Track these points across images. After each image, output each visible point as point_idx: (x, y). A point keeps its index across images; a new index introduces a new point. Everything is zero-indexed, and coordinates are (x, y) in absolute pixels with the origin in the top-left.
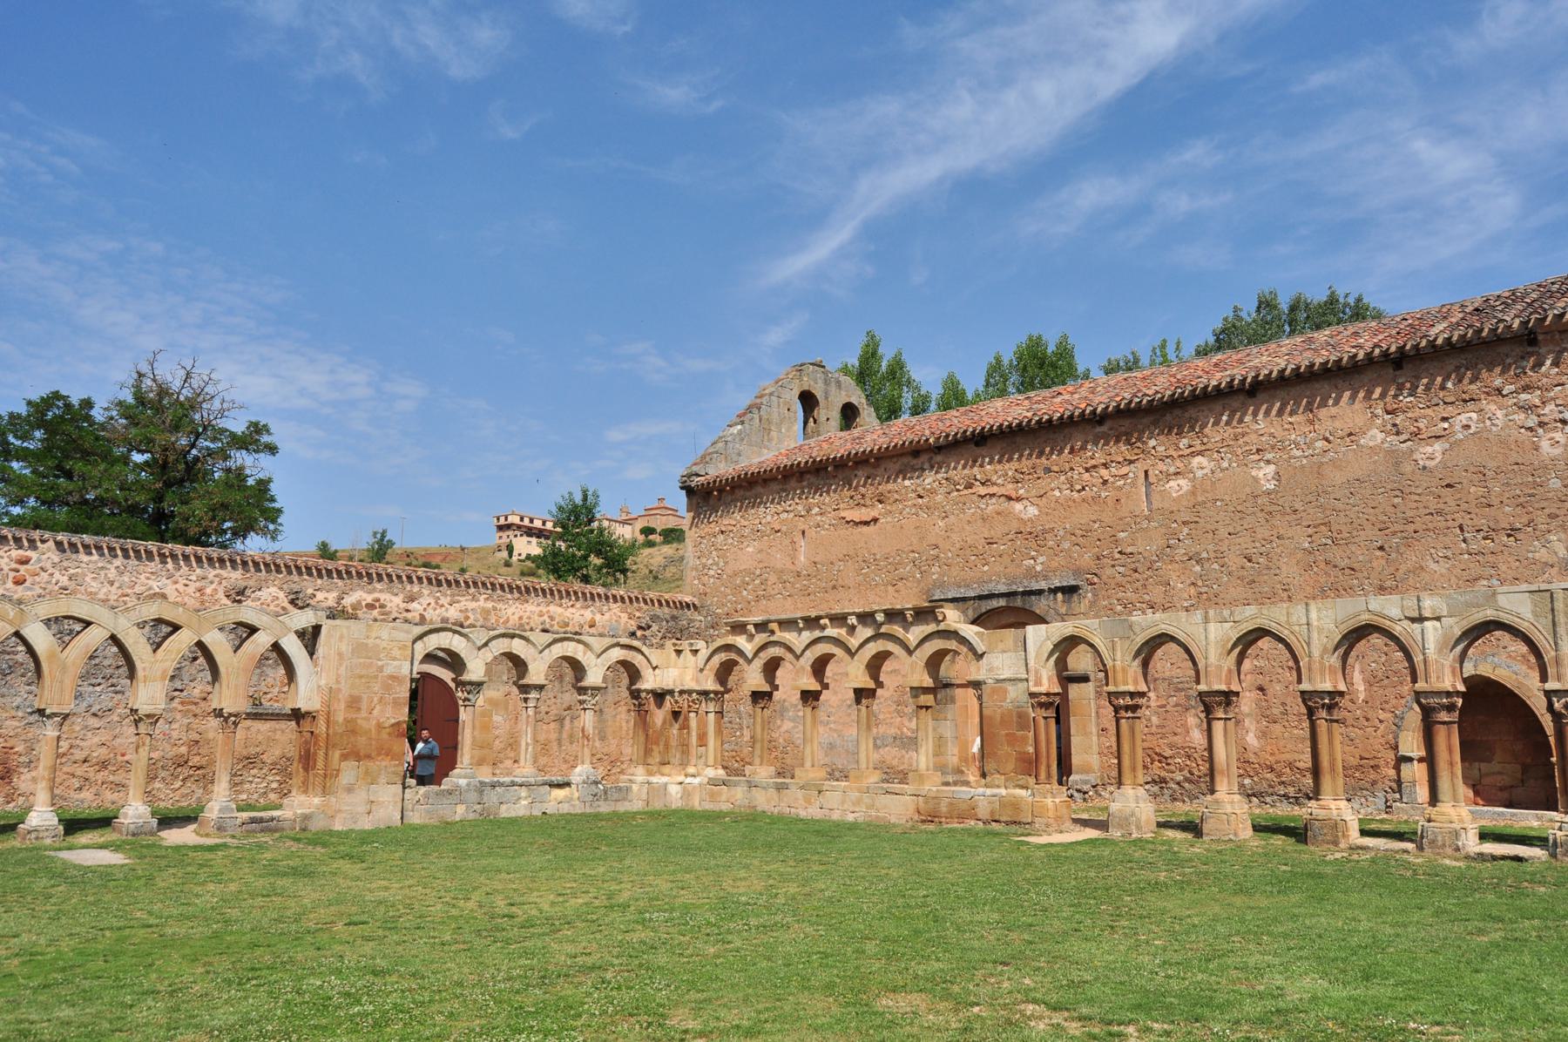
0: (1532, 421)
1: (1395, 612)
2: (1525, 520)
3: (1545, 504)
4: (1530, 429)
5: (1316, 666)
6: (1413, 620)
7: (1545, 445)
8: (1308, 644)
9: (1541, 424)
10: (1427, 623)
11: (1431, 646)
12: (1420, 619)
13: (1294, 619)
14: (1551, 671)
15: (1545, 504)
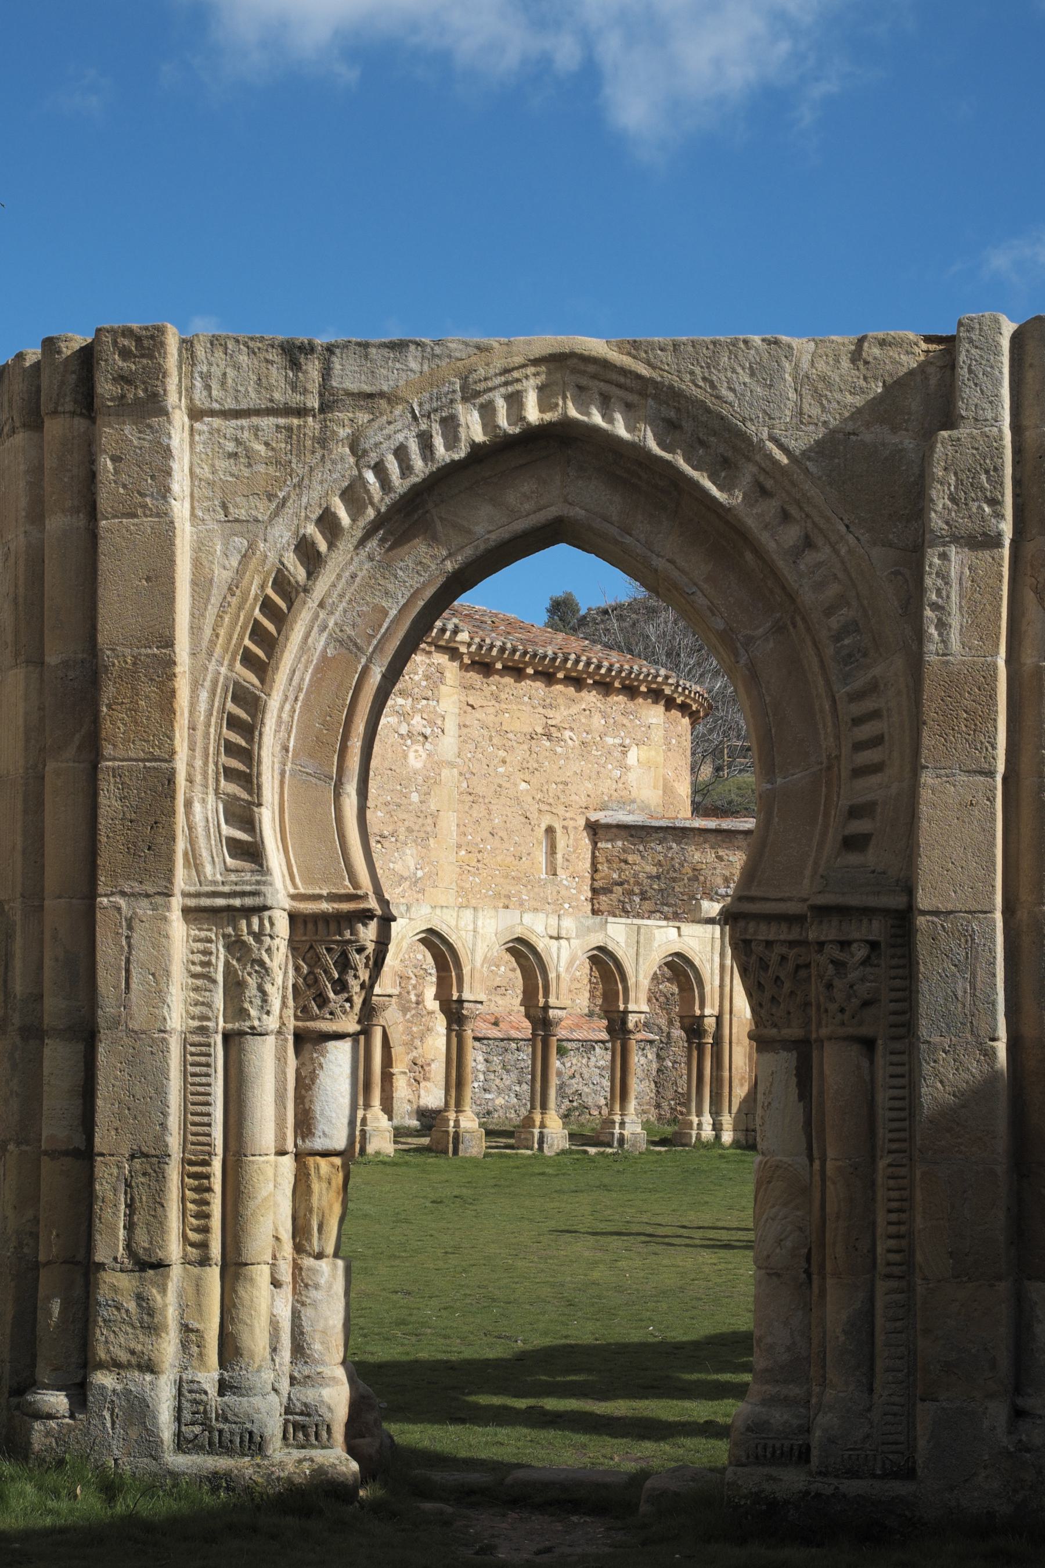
0: (403, 729)
1: (540, 929)
2: (390, 829)
3: (405, 816)
4: (401, 736)
5: (477, 975)
6: (551, 937)
7: (411, 755)
8: (473, 952)
9: (410, 735)
10: (563, 942)
11: (563, 963)
12: (558, 938)
13: (462, 924)
14: (632, 995)
15: (405, 816)
